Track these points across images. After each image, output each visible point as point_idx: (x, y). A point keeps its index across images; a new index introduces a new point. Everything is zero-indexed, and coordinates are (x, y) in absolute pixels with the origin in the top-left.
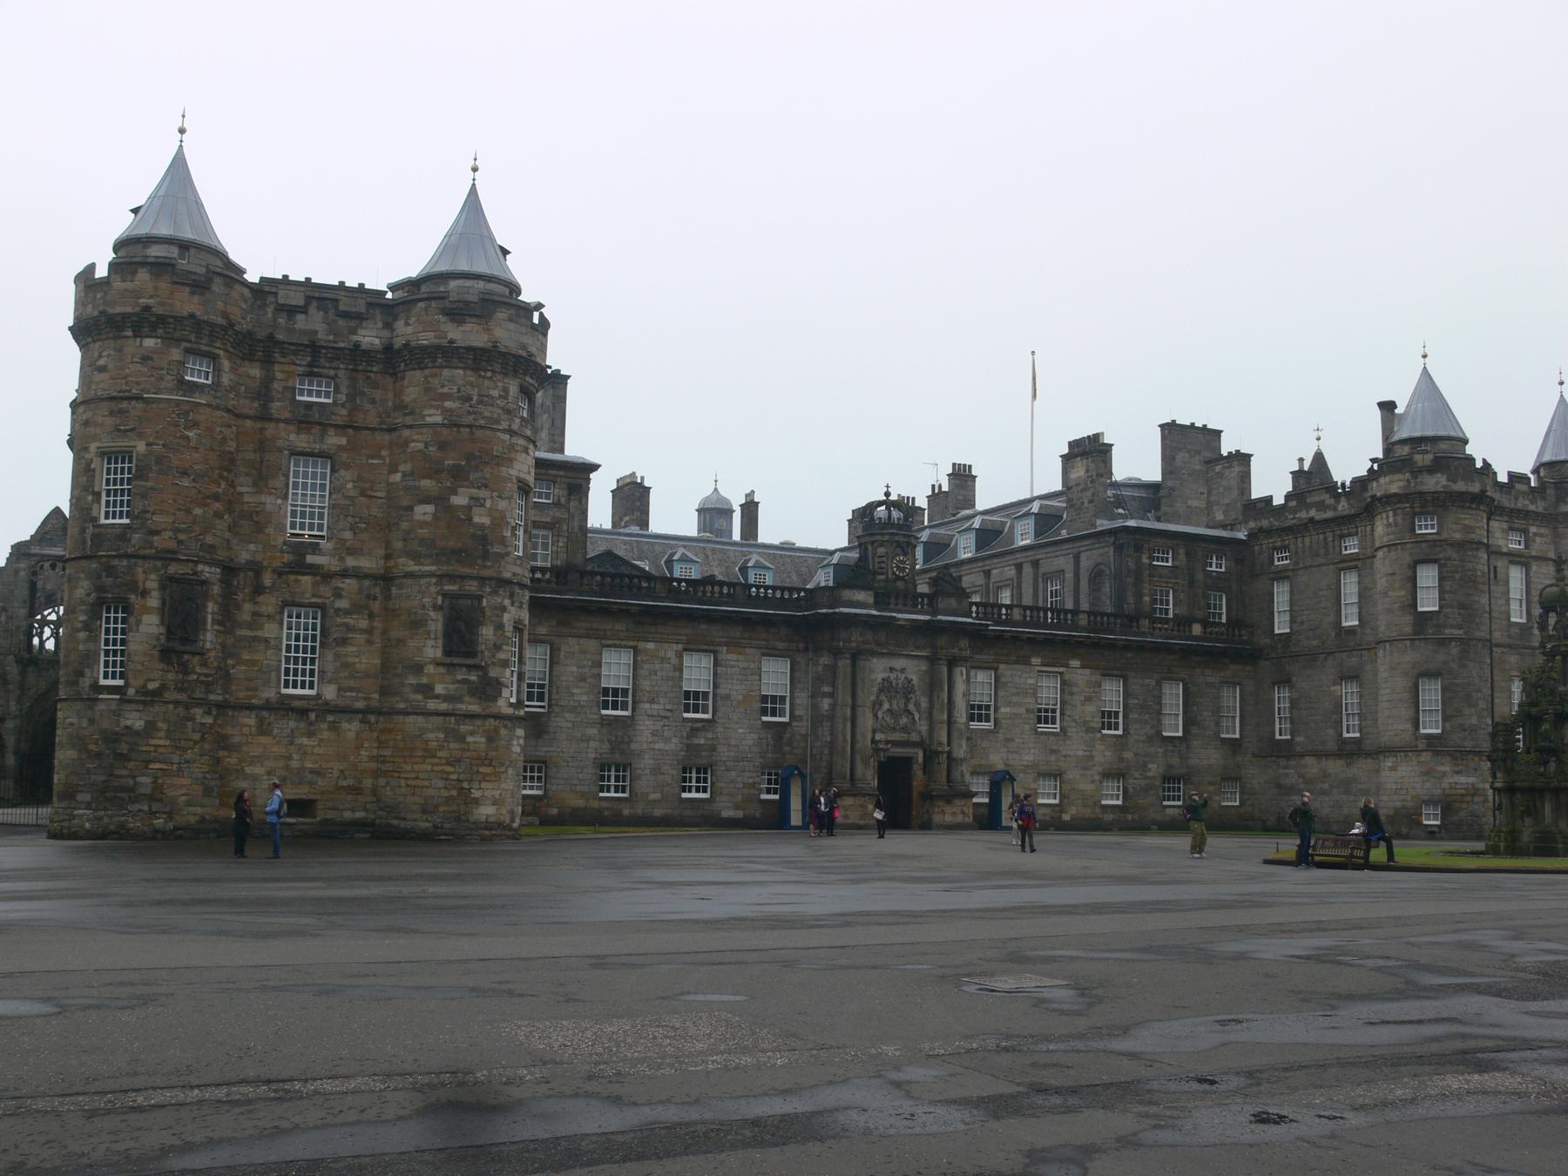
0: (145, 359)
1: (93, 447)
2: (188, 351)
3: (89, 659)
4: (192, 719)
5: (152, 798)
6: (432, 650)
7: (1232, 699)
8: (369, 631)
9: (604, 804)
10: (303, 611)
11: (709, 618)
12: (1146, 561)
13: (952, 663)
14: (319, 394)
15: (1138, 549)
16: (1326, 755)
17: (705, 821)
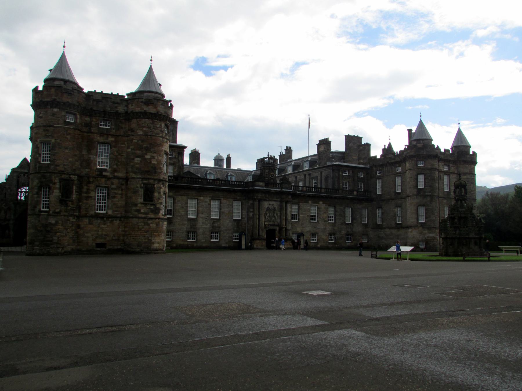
0: (54, 114)
1: (39, 140)
2: (67, 113)
3: (38, 203)
4: (69, 220)
5: (57, 243)
6: (141, 200)
7: (365, 212)
8: (122, 194)
9: (189, 243)
10: (102, 188)
11: (218, 190)
12: (341, 174)
13: (287, 202)
14: (106, 126)
15: (339, 170)
16: (392, 228)
17: (217, 248)
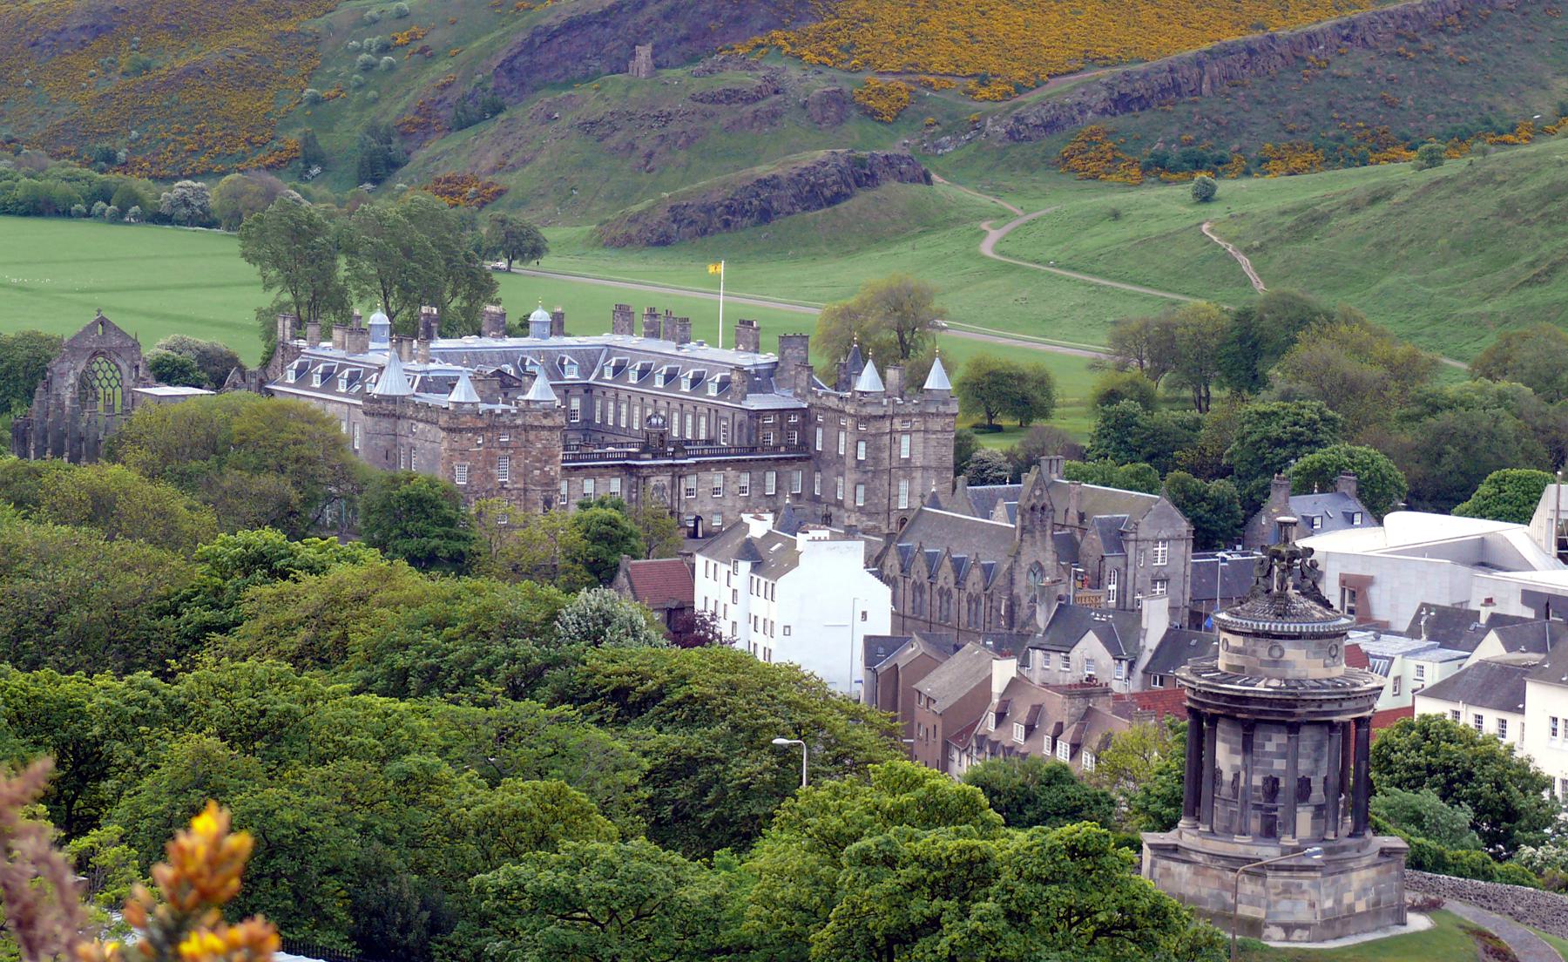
6: (540, 511)
7: (798, 477)
